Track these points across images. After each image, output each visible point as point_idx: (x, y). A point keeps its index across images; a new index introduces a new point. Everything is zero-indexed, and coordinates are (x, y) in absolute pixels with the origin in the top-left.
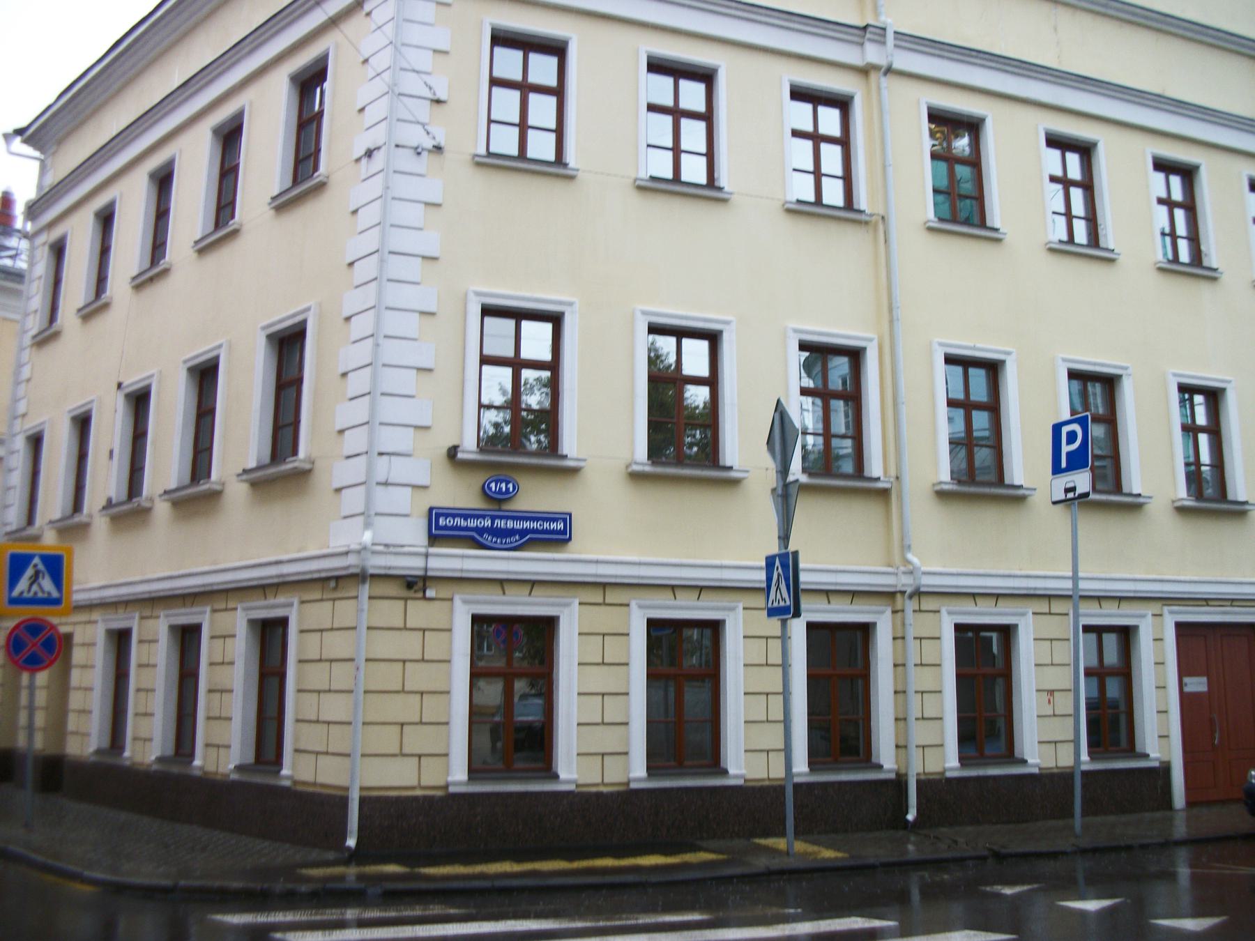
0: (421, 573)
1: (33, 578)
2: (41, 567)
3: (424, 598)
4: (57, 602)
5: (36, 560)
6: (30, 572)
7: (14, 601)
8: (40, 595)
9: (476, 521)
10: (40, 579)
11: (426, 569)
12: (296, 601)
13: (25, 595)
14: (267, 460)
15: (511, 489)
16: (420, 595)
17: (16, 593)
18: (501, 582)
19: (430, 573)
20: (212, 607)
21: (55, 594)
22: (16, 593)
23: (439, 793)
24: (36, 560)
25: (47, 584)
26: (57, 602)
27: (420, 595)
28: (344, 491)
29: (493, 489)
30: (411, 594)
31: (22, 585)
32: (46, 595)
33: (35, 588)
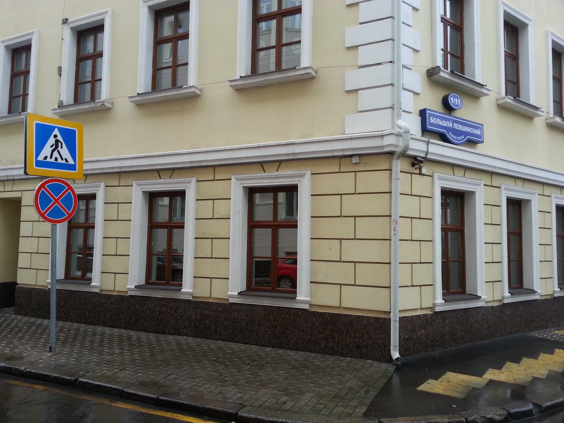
0: (423, 155)
1: (54, 147)
2: (60, 138)
3: (421, 174)
4: (73, 167)
5: (56, 132)
6: (52, 141)
7: (39, 164)
8: (60, 160)
9: (437, 123)
10: (59, 148)
11: (427, 153)
12: (308, 173)
13: (48, 159)
14: (150, 90)
15: (460, 104)
16: (417, 171)
17: (41, 158)
18: (453, 166)
19: (429, 156)
20: (197, 179)
21: (71, 162)
22: (41, 158)
23: (428, 312)
24: (56, 132)
25: (65, 152)
26: (73, 167)
27: (417, 171)
28: (360, 92)
29: (452, 102)
30: (413, 170)
31: (47, 151)
32: (64, 162)
33: (56, 154)
